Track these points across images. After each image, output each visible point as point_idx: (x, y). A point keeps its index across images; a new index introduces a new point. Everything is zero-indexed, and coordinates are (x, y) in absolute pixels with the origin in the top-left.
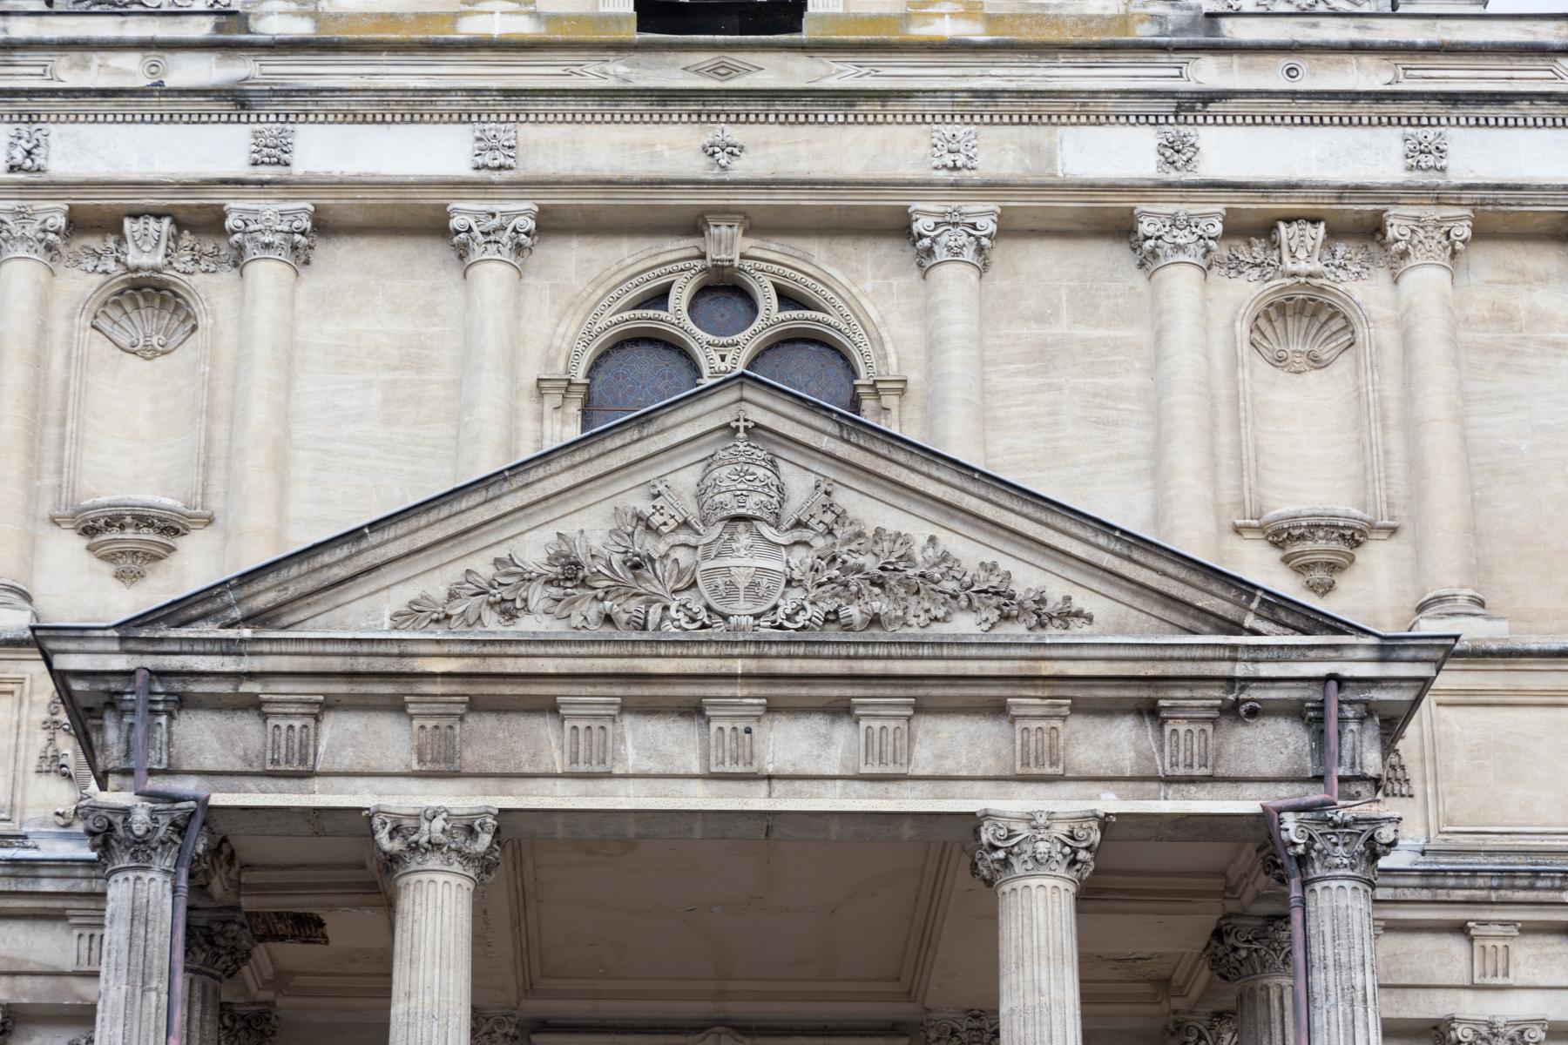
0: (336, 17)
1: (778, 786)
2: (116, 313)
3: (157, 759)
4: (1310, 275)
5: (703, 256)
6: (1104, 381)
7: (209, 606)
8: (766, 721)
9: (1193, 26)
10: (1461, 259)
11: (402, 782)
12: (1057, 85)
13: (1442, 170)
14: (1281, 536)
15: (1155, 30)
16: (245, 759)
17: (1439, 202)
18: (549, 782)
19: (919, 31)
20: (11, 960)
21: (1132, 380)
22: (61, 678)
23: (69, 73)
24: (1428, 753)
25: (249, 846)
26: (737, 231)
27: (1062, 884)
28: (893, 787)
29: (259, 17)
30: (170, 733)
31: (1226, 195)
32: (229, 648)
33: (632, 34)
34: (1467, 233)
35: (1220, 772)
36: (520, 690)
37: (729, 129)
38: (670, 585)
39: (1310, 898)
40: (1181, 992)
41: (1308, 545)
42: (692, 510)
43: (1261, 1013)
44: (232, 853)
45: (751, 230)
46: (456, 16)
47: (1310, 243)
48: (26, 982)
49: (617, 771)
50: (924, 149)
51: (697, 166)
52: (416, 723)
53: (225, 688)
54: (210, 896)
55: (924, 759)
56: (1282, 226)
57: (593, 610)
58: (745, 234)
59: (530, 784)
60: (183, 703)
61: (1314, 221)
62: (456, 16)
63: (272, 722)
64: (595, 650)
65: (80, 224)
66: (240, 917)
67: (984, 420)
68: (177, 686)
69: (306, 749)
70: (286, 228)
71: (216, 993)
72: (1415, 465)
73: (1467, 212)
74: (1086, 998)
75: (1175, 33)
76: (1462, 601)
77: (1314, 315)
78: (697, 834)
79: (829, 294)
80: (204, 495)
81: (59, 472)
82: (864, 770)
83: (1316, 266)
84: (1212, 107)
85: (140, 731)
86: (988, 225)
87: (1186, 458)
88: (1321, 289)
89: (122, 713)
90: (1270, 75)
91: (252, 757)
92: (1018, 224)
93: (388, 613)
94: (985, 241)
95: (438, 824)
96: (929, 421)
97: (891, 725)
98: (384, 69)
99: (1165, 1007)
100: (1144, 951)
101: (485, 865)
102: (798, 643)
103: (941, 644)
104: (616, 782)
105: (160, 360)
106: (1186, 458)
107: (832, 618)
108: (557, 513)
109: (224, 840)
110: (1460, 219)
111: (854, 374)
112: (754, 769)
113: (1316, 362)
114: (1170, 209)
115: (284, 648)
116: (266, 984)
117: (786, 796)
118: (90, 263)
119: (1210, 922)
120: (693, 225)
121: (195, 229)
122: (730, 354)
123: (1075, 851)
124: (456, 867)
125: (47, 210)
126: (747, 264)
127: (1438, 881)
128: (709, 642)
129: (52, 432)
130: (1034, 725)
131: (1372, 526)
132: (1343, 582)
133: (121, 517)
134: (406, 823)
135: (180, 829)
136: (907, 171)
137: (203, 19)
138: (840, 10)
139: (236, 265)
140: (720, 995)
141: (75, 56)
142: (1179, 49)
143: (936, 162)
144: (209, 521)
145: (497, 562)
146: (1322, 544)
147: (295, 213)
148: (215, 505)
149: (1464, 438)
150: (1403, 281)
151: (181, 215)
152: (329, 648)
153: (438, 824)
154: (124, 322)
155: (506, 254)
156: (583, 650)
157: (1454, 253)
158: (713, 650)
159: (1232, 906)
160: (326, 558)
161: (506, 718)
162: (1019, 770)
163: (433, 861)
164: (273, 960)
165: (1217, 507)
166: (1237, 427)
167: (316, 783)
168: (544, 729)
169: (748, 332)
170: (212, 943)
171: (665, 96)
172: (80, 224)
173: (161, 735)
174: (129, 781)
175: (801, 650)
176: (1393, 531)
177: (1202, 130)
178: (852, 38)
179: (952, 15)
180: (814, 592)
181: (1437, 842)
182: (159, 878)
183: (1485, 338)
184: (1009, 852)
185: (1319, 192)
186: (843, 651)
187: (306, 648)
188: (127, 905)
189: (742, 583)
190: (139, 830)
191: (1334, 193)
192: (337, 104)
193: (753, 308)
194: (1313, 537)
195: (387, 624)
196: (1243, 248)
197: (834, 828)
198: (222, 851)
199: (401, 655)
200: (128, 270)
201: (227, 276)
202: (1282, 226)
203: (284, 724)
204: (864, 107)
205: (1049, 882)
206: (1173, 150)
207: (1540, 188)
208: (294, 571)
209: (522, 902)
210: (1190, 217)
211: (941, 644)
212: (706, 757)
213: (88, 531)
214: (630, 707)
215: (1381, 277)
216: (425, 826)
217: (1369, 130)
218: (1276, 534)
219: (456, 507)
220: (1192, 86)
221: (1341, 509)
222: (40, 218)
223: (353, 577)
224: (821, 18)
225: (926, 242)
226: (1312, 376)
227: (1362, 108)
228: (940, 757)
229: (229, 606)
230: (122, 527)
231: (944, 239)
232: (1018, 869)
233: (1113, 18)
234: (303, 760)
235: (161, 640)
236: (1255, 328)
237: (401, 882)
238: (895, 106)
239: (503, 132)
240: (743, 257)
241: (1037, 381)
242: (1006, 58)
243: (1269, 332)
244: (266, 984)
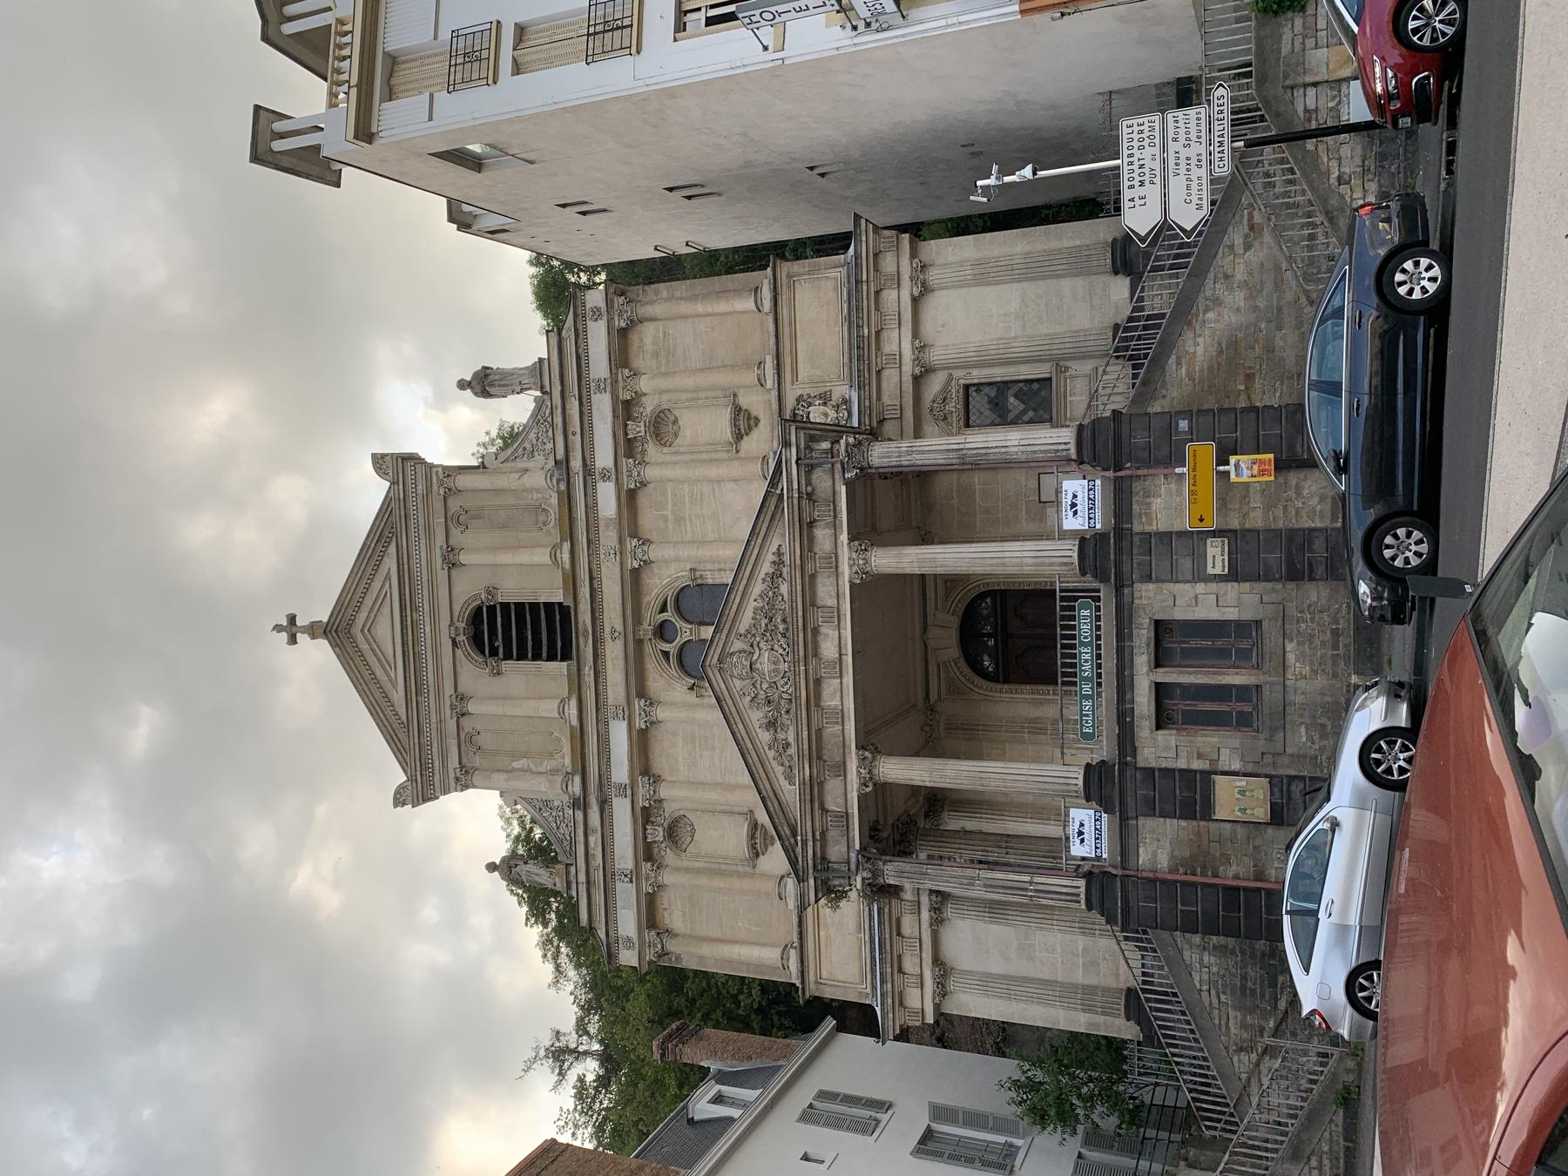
1: (843, 652)
61: (626, 425)
83: (642, 424)
84: (588, 463)
95: (862, 771)
101: (877, 751)
153: (862, 771)
157: (635, 375)
205: (873, 558)
206: (605, 476)
232: (869, 569)
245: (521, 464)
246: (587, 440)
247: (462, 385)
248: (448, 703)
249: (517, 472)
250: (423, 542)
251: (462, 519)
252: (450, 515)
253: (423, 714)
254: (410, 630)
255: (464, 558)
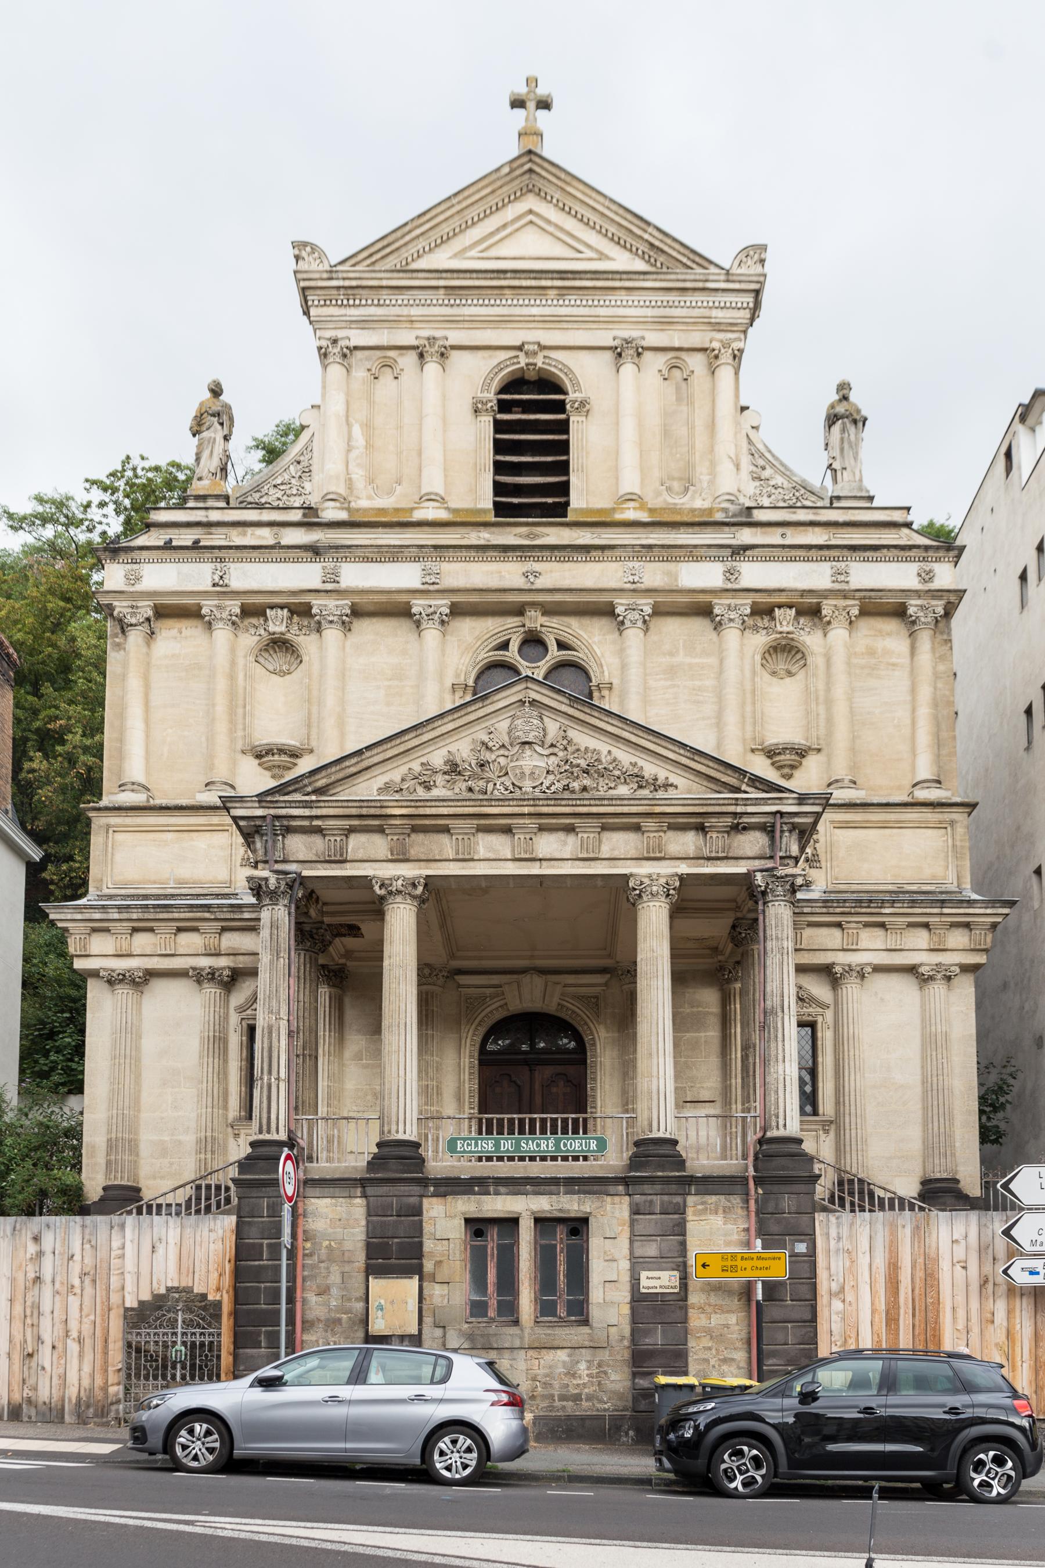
0: (358, 510)
2: (266, 655)
3: (279, 855)
4: (788, 633)
5: (524, 626)
6: (698, 683)
7: (297, 786)
8: (539, 834)
9: (740, 513)
10: (855, 625)
11: (385, 864)
12: (680, 542)
13: (847, 582)
14: (771, 753)
15: (724, 515)
16: (317, 855)
17: (845, 597)
18: (447, 863)
19: (619, 516)
20: (234, 948)
21: (710, 683)
22: (235, 819)
23: (237, 538)
24: (829, 849)
25: (326, 894)
26: (539, 613)
27: (663, 905)
28: (592, 863)
29: (323, 510)
30: (283, 844)
31: (752, 594)
32: (307, 805)
33: (492, 519)
34: (857, 612)
35: (730, 855)
36: (433, 822)
37: (534, 564)
38: (497, 774)
39: (767, 909)
40: (722, 953)
41: (782, 757)
42: (506, 740)
43: (750, 961)
44: (318, 898)
45: (545, 613)
46: (412, 509)
47: (788, 618)
48: (241, 958)
49: (476, 858)
50: (620, 574)
51: (520, 582)
52: (389, 838)
53: (306, 823)
54: (310, 917)
55: (605, 851)
56: (776, 609)
57: (464, 786)
58: (543, 615)
59: (439, 864)
60: (289, 830)
61: (790, 607)
62: (412, 509)
63: (327, 838)
64: (464, 803)
65: (247, 612)
66: (324, 926)
67: (646, 701)
68: (285, 823)
69: (343, 850)
70: (339, 613)
71: (316, 960)
72: (830, 721)
73: (857, 602)
74: (673, 956)
75: (732, 517)
76: (846, 782)
77: (789, 652)
78: (511, 885)
79: (579, 643)
80: (308, 739)
81: (244, 729)
82: (580, 856)
83: (791, 628)
84: (748, 553)
85: (270, 843)
86: (648, 610)
87: (731, 718)
88: (792, 639)
89: (262, 835)
90: (774, 537)
91: (320, 853)
92: (663, 609)
93: (375, 788)
94: (647, 618)
95: (400, 882)
96: (622, 703)
97: (592, 835)
98: (380, 536)
99: (716, 960)
100: (706, 935)
101: (422, 901)
102: (551, 799)
103: (612, 799)
104: (476, 863)
105: (287, 677)
106: (731, 718)
107: (566, 788)
108: (448, 741)
109: (313, 892)
110: (853, 606)
111: (591, 681)
112: (533, 856)
113: (790, 674)
114: (727, 602)
115: (330, 804)
116: (342, 956)
117: (548, 867)
118: (253, 631)
119: (730, 921)
120: (519, 610)
121: (299, 614)
122: (536, 671)
123: (668, 890)
124: (409, 901)
125: (231, 605)
126: (543, 629)
127: (829, 904)
128: (513, 799)
129: (240, 711)
130: (652, 835)
131: (810, 748)
132: (797, 774)
133: (272, 750)
134: (386, 882)
135: (290, 886)
136: (613, 584)
137: (298, 511)
138: (585, 506)
139: (318, 631)
140: (532, 957)
141: (240, 529)
142: (734, 524)
143: (626, 580)
144: (311, 751)
145: (422, 764)
146: (788, 757)
147: (342, 606)
148: (314, 744)
149: (851, 708)
150: (828, 635)
151: (293, 607)
152: (350, 804)
153: (400, 882)
154: (270, 659)
155: (437, 625)
156: (459, 804)
157: (851, 622)
158: (515, 803)
159: (739, 915)
160: (347, 763)
161: (428, 835)
162: (646, 855)
163: (399, 899)
164: (344, 946)
165: (744, 740)
166: (754, 704)
167: (348, 865)
168: (444, 839)
169: (544, 661)
170: (313, 938)
171: (506, 548)
172: (247, 612)
173: (280, 845)
174: (267, 866)
175: (552, 802)
176: (819, 750)
177: (743, 564)
178: (589, 520)
179: (634, 508)
180: (558, 776)
181: (831, 888)
182: (282, 908)
183: (863, 662)
184: (641, 891)
185: (793, 593)
186: (570, 803)
187: (340, 804)
188: (269, 920)
189: (527, 772)
190: (272, 887)
191: (799, 593)
192: (359, 552)
193: (546, 649)
194: (784, 754)
195: (375, 793)
196: (759, 620)
197: (569, 881)
198: (311, 896)
199: (381, 807)
200: (270, 634)
201: (314, 636)
202: (776, 609)
203: (332, 839)
204: (594, 553)
206: (730, 574)
207: (890, 591)
208: (334, 769)
209: (444, 919)
210: (736, 606)
211: (612, 799)
212: (513, 851)
213: (259, 756)
214: (481, 829)
215: (819, 633)
216: (394, 883)
217: (816, 564)
218: (769, 752)
219: (403, 739)
220: (739, 542)
221: (796, 741)
222: (229, 609)
223: (360, 772)
224: (576, 510)
225: (621, 618)
226: (788, 680)
227: (813, 553)
228: (613, 850)
229: (306, 786)
230: (273, 754)
231: (628, 617)
233: (705, 510)
234: (341, 855)
235: (277, 802)
236: (764, 658)
237: (386, 908)
238: (608, 553)
239: (433, 566)
240: (542, 626)
241: (669, 683)
242: (658, 529)
243: (770, 660)
244: (342, 956)
245: (745, 461)
246: (777, 552)
247: (844, 390)
248: (438, 334)
249: (737, 456)
250: (649, 312)
251: (676, 373)
252: (683, 355)
253: (421, 295)
254: (533, 283)
255: (628, 369)
